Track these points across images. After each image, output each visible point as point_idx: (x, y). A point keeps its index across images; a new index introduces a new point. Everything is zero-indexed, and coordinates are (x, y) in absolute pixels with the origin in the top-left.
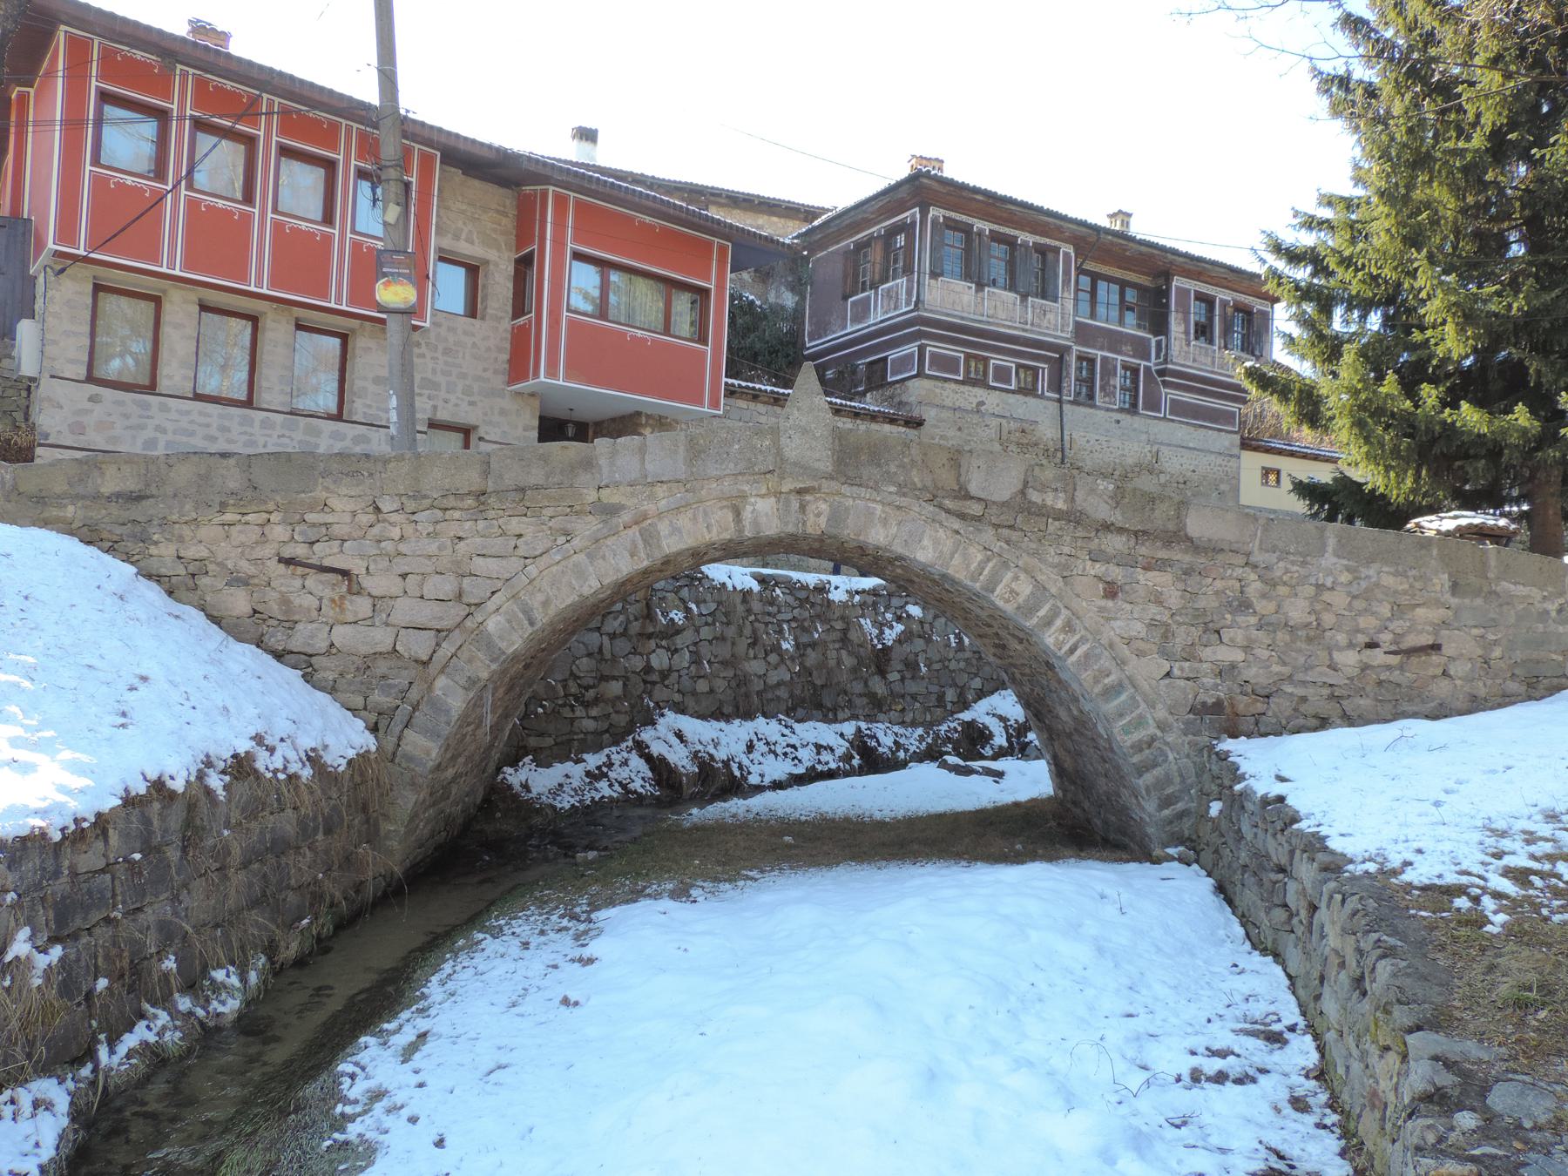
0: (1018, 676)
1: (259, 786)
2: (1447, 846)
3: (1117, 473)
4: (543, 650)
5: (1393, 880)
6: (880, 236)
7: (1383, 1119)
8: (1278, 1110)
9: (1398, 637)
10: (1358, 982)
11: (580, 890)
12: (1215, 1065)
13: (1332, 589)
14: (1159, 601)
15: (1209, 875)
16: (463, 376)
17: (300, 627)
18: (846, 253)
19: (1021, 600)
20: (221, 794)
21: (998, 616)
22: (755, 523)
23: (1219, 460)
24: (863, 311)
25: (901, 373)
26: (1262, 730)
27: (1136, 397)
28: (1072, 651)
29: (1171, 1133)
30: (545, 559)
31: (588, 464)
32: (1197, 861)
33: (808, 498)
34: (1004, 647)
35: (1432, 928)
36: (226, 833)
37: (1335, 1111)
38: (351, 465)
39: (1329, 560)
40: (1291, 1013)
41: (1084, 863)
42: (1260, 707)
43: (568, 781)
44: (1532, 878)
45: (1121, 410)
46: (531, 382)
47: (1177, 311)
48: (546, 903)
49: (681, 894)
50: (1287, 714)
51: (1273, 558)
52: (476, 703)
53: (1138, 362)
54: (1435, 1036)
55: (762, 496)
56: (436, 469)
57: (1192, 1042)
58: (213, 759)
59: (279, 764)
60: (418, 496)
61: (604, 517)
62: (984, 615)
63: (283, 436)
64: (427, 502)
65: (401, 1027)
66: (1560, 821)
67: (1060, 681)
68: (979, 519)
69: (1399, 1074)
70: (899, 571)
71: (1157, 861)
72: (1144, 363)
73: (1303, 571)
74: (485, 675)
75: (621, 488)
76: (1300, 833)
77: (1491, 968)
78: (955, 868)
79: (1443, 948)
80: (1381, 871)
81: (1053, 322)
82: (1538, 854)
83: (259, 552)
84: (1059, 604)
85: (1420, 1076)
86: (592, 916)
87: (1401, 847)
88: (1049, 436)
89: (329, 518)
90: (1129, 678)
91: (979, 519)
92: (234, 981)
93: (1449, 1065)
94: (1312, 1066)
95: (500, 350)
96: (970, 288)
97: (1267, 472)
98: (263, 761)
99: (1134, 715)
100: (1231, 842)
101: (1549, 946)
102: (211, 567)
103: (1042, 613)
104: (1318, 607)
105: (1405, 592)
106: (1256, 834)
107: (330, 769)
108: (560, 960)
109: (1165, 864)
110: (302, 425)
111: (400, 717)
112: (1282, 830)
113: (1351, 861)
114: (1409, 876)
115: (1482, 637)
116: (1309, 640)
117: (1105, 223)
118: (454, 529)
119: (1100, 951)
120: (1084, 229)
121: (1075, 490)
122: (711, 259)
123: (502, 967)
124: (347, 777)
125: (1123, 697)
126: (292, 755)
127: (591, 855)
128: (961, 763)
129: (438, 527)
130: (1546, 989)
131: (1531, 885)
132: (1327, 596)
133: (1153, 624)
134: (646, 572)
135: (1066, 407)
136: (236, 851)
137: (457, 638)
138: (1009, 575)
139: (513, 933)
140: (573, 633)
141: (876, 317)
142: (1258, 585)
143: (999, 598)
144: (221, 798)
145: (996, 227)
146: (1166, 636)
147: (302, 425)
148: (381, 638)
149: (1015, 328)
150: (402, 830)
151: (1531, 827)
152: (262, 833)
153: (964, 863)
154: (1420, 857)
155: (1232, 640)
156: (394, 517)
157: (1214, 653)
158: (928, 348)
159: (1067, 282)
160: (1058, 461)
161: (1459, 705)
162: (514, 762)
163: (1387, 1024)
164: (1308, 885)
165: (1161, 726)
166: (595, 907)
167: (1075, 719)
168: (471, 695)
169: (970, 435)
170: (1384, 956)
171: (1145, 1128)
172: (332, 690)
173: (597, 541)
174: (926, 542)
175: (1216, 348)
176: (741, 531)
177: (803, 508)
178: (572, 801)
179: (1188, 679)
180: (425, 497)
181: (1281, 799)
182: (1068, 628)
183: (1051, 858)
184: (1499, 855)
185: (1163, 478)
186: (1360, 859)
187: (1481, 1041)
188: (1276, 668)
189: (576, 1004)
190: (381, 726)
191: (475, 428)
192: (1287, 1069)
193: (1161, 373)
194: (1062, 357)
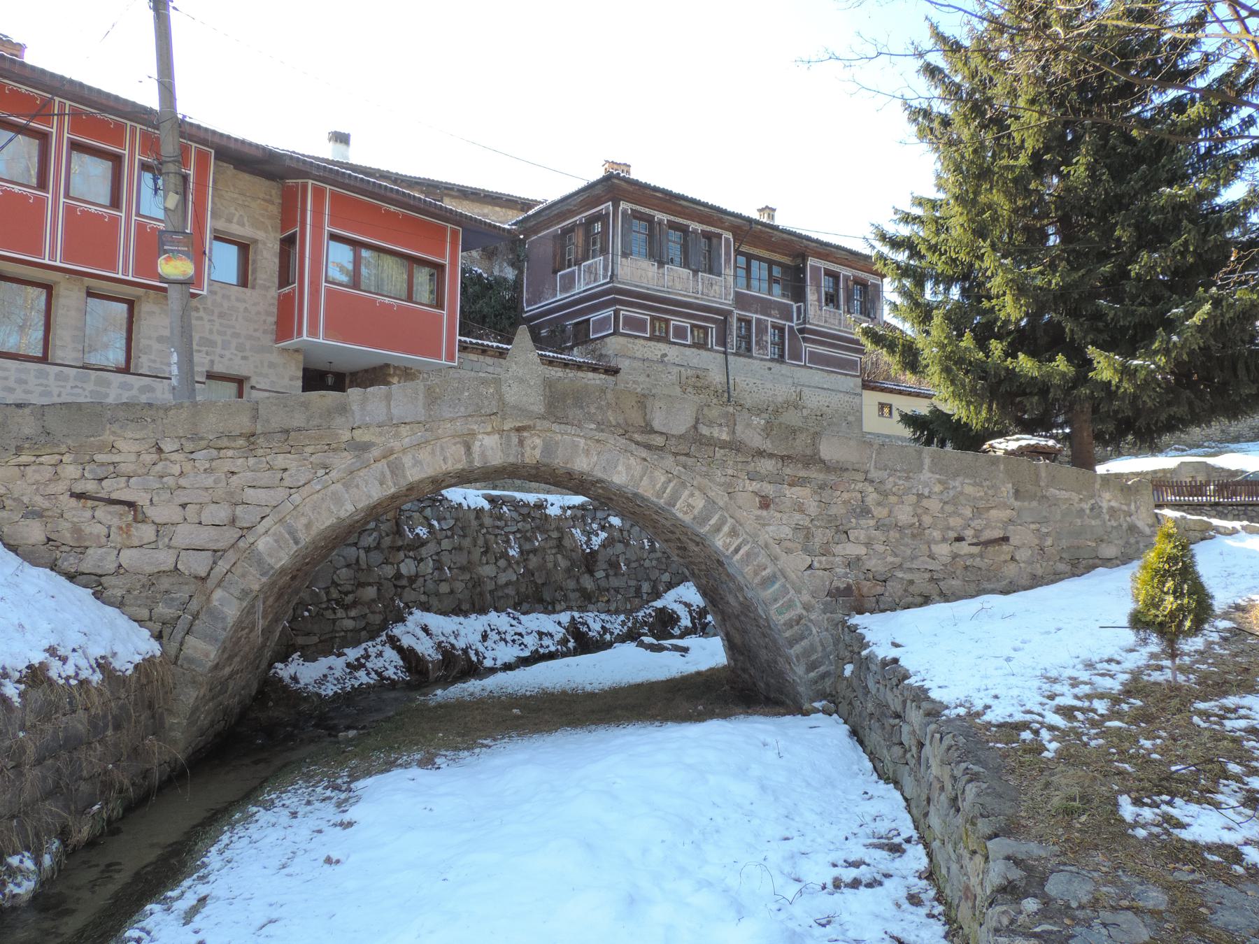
0: (696, 571)
1: (52, 691)
2: (1015, 692)
3: (770, 409)
4: (307, 564)
5: (977, 721)
6: (581, 224)
7: (974, 907)
8: (898, 906)
9: (978, 532)
10: (954, 800)
11: (341, 764)
12: (851, 874)
13: (929, 497)
14: (801, 509)
15: (846, 723)
17: (90, 551)
18: (555, 236)
19: (696, 512)
20: (16, 700)
21: (679, 525)
22: (483, 455)
23: (847, 398)
24: (569, 283)
25: (601, 332)
26: (882, 607)
27: (783, 350)
28: (737, 551)
29: (818, 931)
31: (343, 409)
32: (836, 712)
33: (525, 434)
34: (685, 549)
35: (1005, 756)
36: (21, 734)
37: (940, 903)
38: (135, 413)
39: (926, 475)
40: (907, 828)
41: (751, 718)
42: (879, 590)
43: (332, 672)
44: (1076, 713)
45: (772, 360)
46: (295, 340)
48: (312, 777)
49: (428, 762)
50: (899, 594)
51: (884, 474)
52: (250, 611)
54: (1008, 841)
55: (488, 434)
56: (211, 415)
57: (833, 857)
58: (9, 670)
59: (71, 672)
60: (196, 437)
61: (357, 453)
62: (668, 524)
63: (76, 387)
64: (204, 443)
65: (183, 893)
66: (1095, 669)
67: (728, 575)
68: (661, 449)
69: (983, 872)
70: (600, 491)
71: (806, 713)
72: (788, 323)
74: (256, 587)
75: (371, 429)
76: (910, 687)
77: (1047, 785)
78: (650, 728)
79: (1013, 771)
80: (969, 714)
81: (718, 292)
82: (1080, 695)
83: (52, 489)
84: (726, 514)
85: (997, 873)
86: (352, 786)
87: (982, 694)
88: (718, 380)
89: (116, 458)
90: (780, 570)
91: (661, 449)
92: (29, 864)
93: (1018, 863)
94: (923, 869)
95: (268, 314)
97: (882, 406)
98: (56, 670)
99: (785, 599)
100: (860, 696)
101: (1088, 765)
102: (8, 502)
103: (712, 522)
104: (919, 511)
105: (981, 498)
106: (878, 689)
107: (118, 673)
108: (323, 825)
109: (813, 716)
110: (93, 378)
111: (182, 625)
112: (897, 685)
113: (947, 707)
114: (989, 717)
115: (1038, 530)
116: (914, 536)
117: (755, 215)
118: (228, 465)
119: (763, 788)
120: (740, 221)
121: (735, 424)
122: (445, 241)
123: (273, 835)
124: (134, 679)
125: (777, 586)
126: (83, 663)
127: (352, 733)
128: (655, 642)
129: (214, 464)
130: (1086, 799)
131: (1075, 718)
132: (925, 503)
133: (797, 528)
134: (393, 497)
135: (730, 358)
136: (31, 750)
137: (231, 556)
138: (686, 493)
139: (283, 805)
140: (333, 548)
141: (580, 288)
142: (875, 495)
143: (679, 511)
144: (17, 704)
145: (672, 218)
147: (93, 378)
148: (165, 559)
149: (689, 297)
150: (185, 722)
151: (1075, 674)
152: (55, 732)
153: (657, 723)
154: (996, 701)
155: (857, 538)
156: (175, 456)
157: (844, 549)
158: (622, 312)
159: (728, 260)
160: (725, 399)
161: (1024, 582)
162: (284, 659)
163: (974, 833)
164: (917, 728)
165: (807, 607)
166: (354, 778)
167: (741, 604)
168: (245, 604)
169: (656, 380)
170: (970, 781)
171: (798, 929)
172: (120, 605)
173: (352, 472)
174: (620, 468)
175: (841, 312)
176: (471, 462)
178: (335, 689)
179: (825, 570)
180: (202, 439)
181: (895, 661)
182: (733, 533)
183: (725, 716)
184: (1052, 697)
185: (805, 412)
186: (954, 705)
187: (1040, 842)
188: (890, 559)
189: (338, 862)
190: (165, 634)
191: (248, 378)
192: (905, 873)
193: (802, 331)
194: (726, 318)
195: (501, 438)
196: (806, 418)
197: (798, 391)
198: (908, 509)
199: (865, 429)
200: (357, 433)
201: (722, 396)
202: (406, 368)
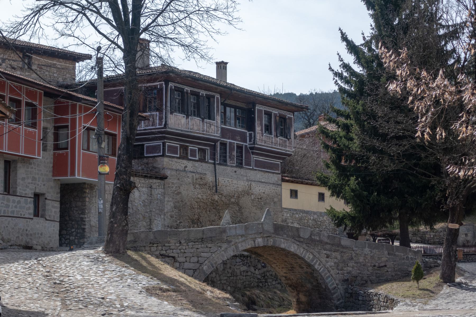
3: (236, 195)
16: (42, 174)
19: (311, 259)
22: (258, 243)
23: (273, 188)
25: (153, 153)
45: (237, 166)
46: (69, 177)
47: (258, 120)
51: (357, 249)
53: (242, 143)
55: (259, 238)
68: (302, 242)
73: (362, 252)
81: (213, 129)
88: (210, 180)
89: (170, 245)
91: (302, 242)
96: (184, 117)
97: (292, 191)
103: (314, 261)
104: (365, 258)
118: (196, 246)
120: (226, 89)
122: (117, 124)
133: (335, 263)
135: (217, 166)
138: (308, 254)
145: (192, 89)
146: (338, 266)
149: (200, 133)
156: (185, 244)
158: (167, 143)
160: (214, 191)
174: (292, 247)
175: (273, 136)
177: (268, 240)
182: (319, 265)
185: (253, 197)
188: (358, 271)
191: (43, 194)
193: (252, 148)
194: (215, 144)
195: (263, 239)
197: (249, 183)
198: (362, 258)
199: (284, 206)
200: (228, 238)
201: (213, 189)
202: (91, 184)
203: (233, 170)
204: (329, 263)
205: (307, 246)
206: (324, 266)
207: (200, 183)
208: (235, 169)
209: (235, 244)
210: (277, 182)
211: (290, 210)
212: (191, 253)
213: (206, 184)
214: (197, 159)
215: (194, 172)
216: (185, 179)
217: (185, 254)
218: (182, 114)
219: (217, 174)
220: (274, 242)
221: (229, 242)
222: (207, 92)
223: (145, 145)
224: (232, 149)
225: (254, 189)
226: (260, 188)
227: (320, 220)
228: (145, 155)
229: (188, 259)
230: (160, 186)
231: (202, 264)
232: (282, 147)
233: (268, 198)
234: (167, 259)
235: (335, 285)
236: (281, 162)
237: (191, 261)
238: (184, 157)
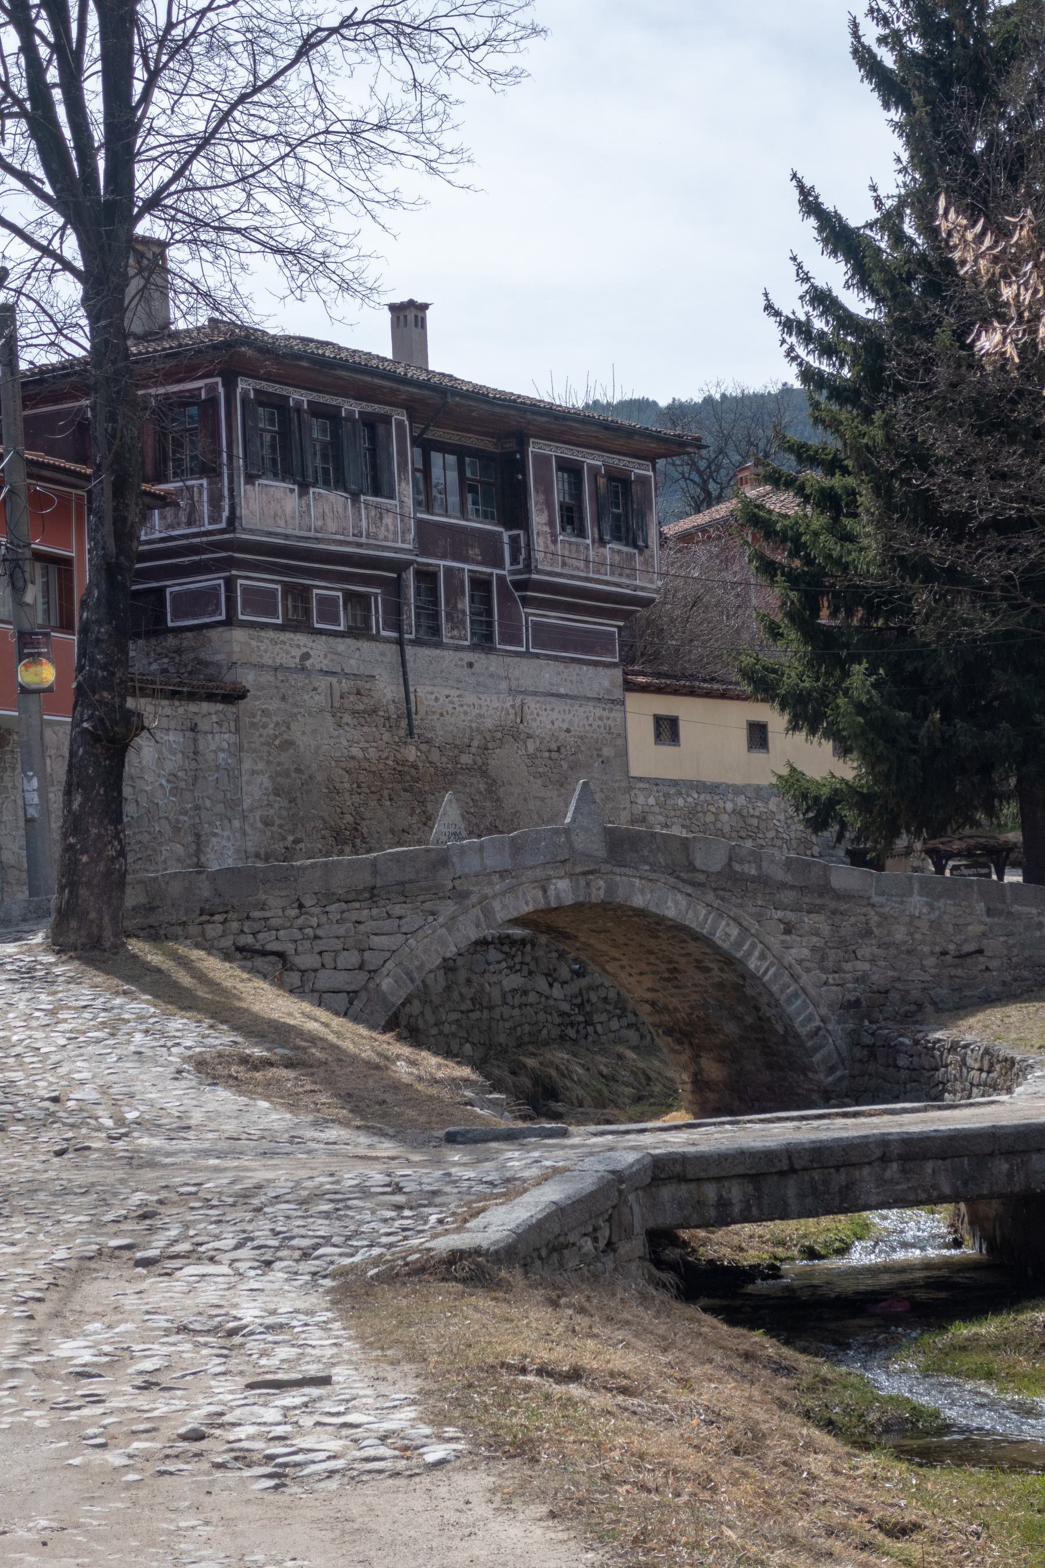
3: (475, 743)
19: (732, 939)
22: (558, 897)
23: (599, 712)
25: (195, 616)
30: (420, 933)
45: (473, 648)
47: (537, 490)
51: (881, 899)
53: (488, 570)
55: (561, 878)
64: (335, 897)
68: (702, 885)
72: (496, 571)
81: (392, 528)
88: (389, 695)
89: (267, 914)
90: (802, 988)
91: (702, 885)
96: (292, 491)
97: (658, 720)
103: (746, 947)
104: (912, 930)
118: (355, 916)
120: (426, 392)
122: (70, 522)
132: (916, 923)
133: (814, 949)
135: (409, 650)
138: (724, 923)
142: (876, 918)
145: (314, 396)
146: (823, 958)
156: (317, 910)
158: (240, 582)
160: (402, 733)
169: (296, 705)
174: (670, 903)
175: (589, 541)
176: (548, 903)
177: (588, 885)
180: (334, 894)
182: (762, 957)
185: (531, 748)
188: (890, 973)
193: (520, 585)
194: (399, 576)
196: (532, 757)
198: (903, 929)
199: (633, 773)
200: (457, 882)
201: (398, 727)
203: (461, 659)
204: (793, 951)
205: (717, 897)
206: (779, 959)
207: (357, 707)
208: (469, 656)
209: (480, 903)
210: (609, 692)
211: (656, 782)
212: (338, 937)
213: (375, 711)
214: (341, 628)
215: (334, 673)
216: (306, 697)
217: (318, 941)
218: (283, 480)
219: (411, 677)
220: (611, 889)
221: (460, 896)
222: (364, 404)
223: (168, 590)
224: (455, 592)
225: (534, 720)
226: (554, 715)
227: (757, 813)
228: (170, 624)
229: (328, 958)
230: (225, 725)
231: (375, 971)
232: (621, 575)
233: (583, 748)
234: (259, 962)
235: (818, 1023)
236: (619, 627)
237: (340, 965)
238: (298, 624)
